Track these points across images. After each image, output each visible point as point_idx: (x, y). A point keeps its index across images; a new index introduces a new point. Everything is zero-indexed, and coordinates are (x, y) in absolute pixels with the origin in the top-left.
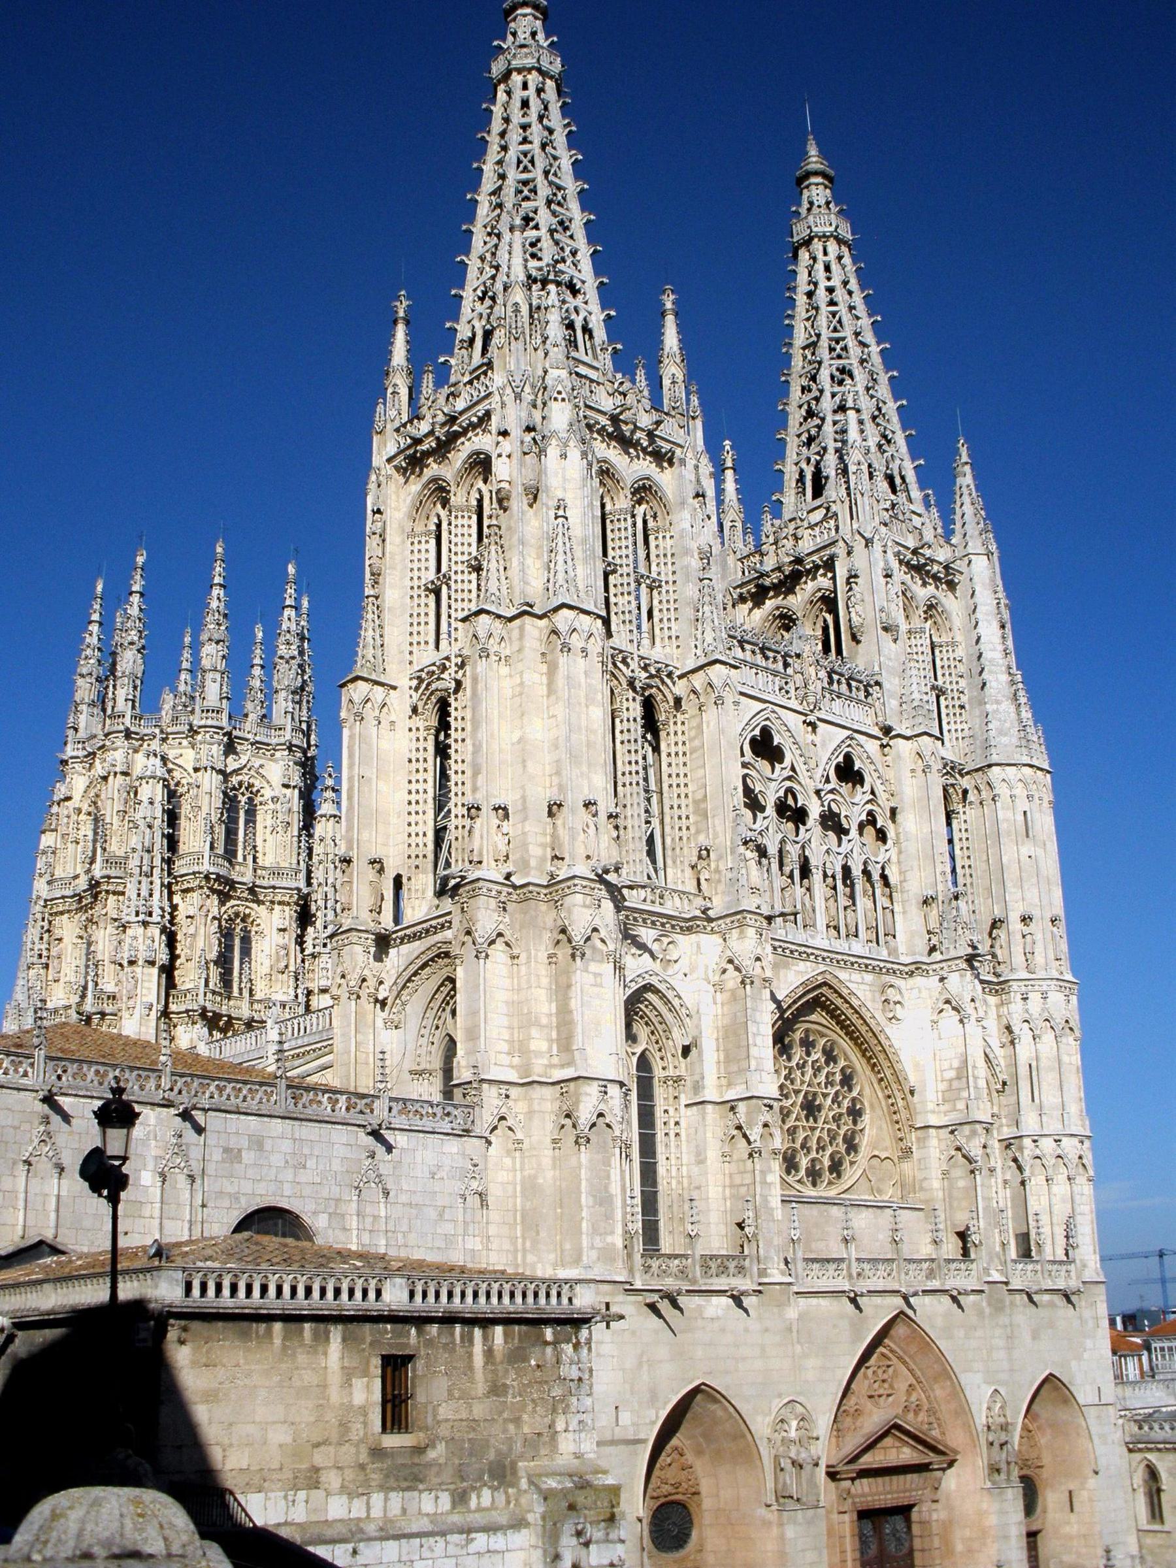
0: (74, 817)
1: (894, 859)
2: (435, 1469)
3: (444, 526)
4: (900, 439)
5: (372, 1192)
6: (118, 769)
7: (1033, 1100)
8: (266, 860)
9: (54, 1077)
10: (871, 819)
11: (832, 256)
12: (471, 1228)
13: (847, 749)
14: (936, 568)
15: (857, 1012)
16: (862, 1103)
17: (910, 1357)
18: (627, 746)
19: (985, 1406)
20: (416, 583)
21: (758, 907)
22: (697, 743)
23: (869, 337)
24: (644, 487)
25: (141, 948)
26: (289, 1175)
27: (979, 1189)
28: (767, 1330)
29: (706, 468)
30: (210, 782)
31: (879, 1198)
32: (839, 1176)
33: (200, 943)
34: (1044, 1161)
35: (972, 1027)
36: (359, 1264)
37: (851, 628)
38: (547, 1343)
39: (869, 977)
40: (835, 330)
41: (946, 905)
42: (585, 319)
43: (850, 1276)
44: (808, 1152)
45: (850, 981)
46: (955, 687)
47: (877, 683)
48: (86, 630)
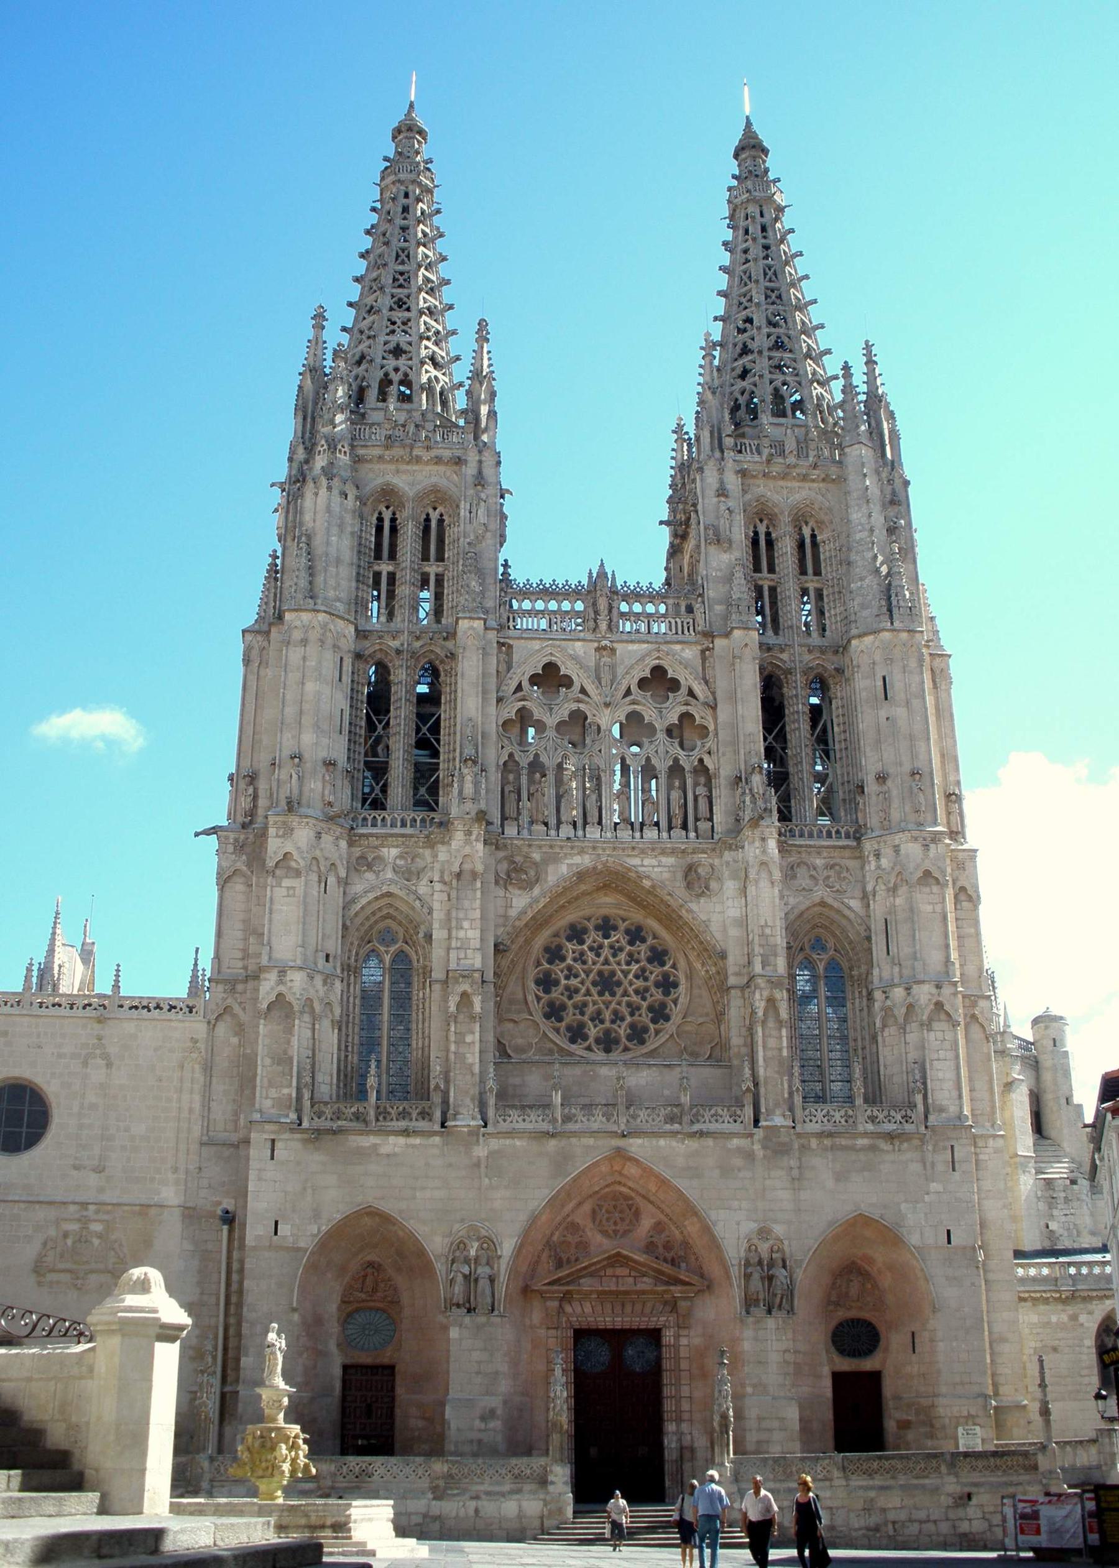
7: (888, 953)
10: (686, 717)
28: (450, 1165)
32: (642, 1042)
39: (670, 860)
40: (746, 285)
45: (643, 866)
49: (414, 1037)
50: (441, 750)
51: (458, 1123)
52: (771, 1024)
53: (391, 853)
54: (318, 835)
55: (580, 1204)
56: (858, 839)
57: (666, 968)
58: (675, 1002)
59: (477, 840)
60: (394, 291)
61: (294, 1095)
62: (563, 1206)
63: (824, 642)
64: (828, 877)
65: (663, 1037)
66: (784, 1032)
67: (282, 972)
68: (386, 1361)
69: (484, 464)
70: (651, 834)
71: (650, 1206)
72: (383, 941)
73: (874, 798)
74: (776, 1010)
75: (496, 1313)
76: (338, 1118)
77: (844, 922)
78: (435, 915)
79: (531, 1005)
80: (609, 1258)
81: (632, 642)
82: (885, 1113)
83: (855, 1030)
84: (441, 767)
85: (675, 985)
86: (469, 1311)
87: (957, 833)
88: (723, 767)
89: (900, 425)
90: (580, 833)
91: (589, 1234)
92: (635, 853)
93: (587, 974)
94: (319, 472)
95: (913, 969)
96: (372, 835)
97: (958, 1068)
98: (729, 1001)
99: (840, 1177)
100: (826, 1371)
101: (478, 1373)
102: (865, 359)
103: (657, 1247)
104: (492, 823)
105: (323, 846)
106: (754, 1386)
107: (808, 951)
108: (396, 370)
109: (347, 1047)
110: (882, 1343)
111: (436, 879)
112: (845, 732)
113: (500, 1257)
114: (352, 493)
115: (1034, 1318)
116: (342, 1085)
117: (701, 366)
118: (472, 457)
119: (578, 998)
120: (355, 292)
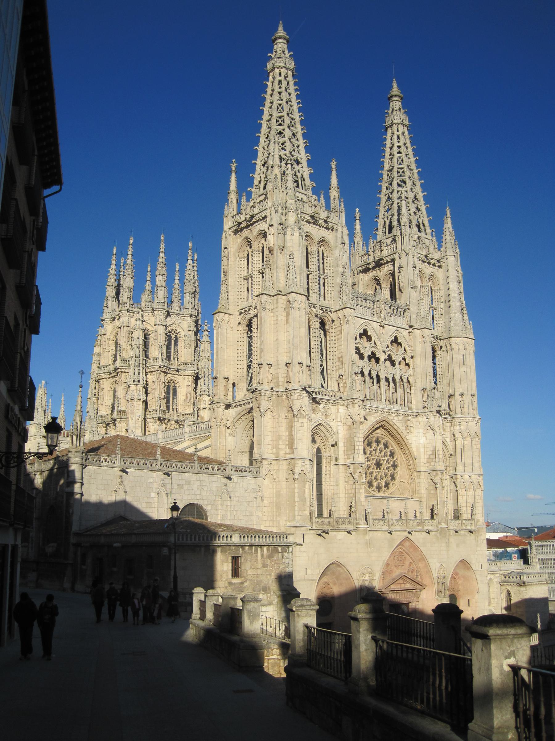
0: (107, 342)
1: (412, 374)
2: (247, 588)
3: (250, 256)
4: (423, 208)
5: (227, 497)
6: (125, 325)
7: (462, 461)
8: (182, 360)
9: (123, 463)
11: (400, 132)
12: (258, 508)
13: (396, 335)
16: (398, 463)
17: (411, 553)
18: (315, 339)
19: (437, 570)
20: (240, 276)
21: (359, 397)
22: (339, 337)
23: (413, 166)
24: (323, 241)
25: (136, 394)
26: (198, 492)
27: (438, 494)
28: (358, 543)
29: (346, 232)
30: (161, 330)
31: (403, 497)
32: (388, 488)
33: (158, 392)
34: (465, 483)
35: (438, 435)
36: (225, 529)
37: (400, 288)
38: (279, 552)
39: (401, 418)
40: (400, 164)
41: (430, 391)
42: (302, 174)
43: (389, 526)
44: (377, 480)
46: (439, 307)
47: (408, 309)
48: (110, 268)
70: (397, 407)
99: (458, 546)
111: (339, 420)
119: (371, 470)
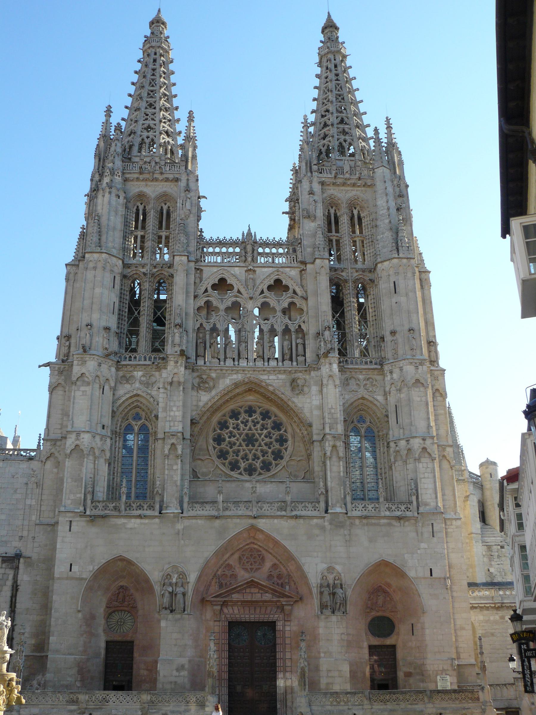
1: (306, 320)
14: (352, 181)
15: (272, 393)
16: (286, 436)
32: (269, 470)
40: (326, 93)
45: (269, 379)
46: (369, 233)
49: (149, 468)
50: (166, 322)
51: (168, 511)
52: (334, 459)
53: (138, 374)
54: (100, 365)
55: (232, 554)
56: (382, 365)
57: (281, 432)
58: (286, 449)
59: (181, 366)
60: (148, 99)
61: (83, 498)
62: (223, 555)
63: (364, 267)
64: (366, 384)
65: (280, 467)
66: (341, 463)
67: (78, 434)
68: (129, 639)
69: (190, 181)
71: (270, 555)
72: (134, 419)
73: (389, 343)
74: (337, 451)
75: (186, 612)
76: (105, 509)
77: (374, 408)
78: (160, 404)
79: (210, 451)
80: (247, 583)
81: (264, 267)
82: (396, 506)
83: (381, 464)
84: (166, 331)
85: (286, 441)
86: (172, 611)
87: (434, 362)
88: (311, 329)
89: (404, 157)
90: (236, 363)
91: (237, 570)
92: (265, 372)
93: (240, 435)
94: (106, 185)
95: (411, 430)
96: (129, 365)
97: (435, 482)
98: (313, 448)
99: (371, 540)
100: (366, 645)
101: (175, 645)
102: (386, 126)
103: (274, 577)
104: (189, 358)
105: (102, 370)
106: (325, 653)
107: (356, 423)
108: (148, 137)
109: (114, 473)
110: (396, 630)
112: (375, 311)
113: (188, 583)
114: (122, 195)
115: (481, 618)
116: (110, 493)
117: (301, 132)
118: (184, 178)
119: (235, 448)
120: (129, 101)
